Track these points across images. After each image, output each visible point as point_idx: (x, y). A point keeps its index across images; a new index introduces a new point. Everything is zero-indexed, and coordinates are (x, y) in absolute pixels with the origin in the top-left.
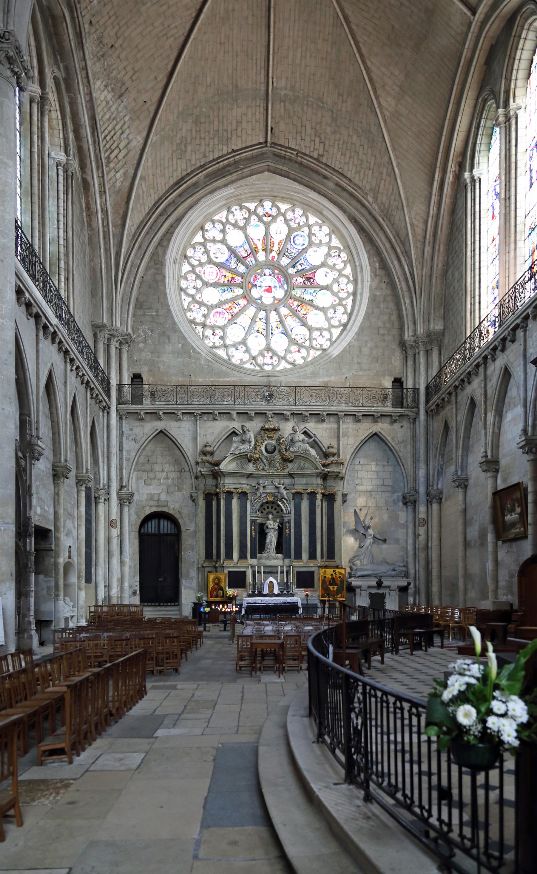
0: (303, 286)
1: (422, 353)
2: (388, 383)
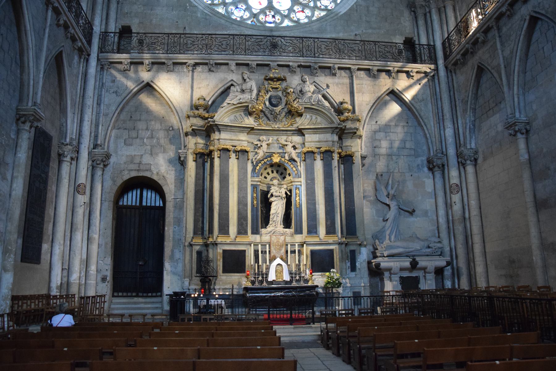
1: (434, 11)
2: (399, 40)
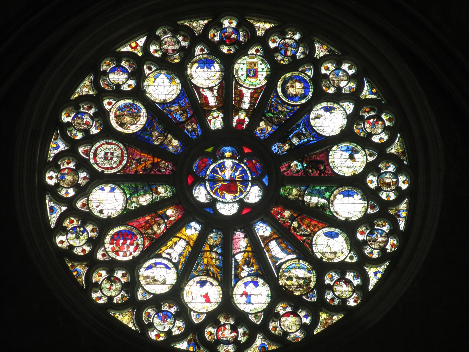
0: (304, 180)
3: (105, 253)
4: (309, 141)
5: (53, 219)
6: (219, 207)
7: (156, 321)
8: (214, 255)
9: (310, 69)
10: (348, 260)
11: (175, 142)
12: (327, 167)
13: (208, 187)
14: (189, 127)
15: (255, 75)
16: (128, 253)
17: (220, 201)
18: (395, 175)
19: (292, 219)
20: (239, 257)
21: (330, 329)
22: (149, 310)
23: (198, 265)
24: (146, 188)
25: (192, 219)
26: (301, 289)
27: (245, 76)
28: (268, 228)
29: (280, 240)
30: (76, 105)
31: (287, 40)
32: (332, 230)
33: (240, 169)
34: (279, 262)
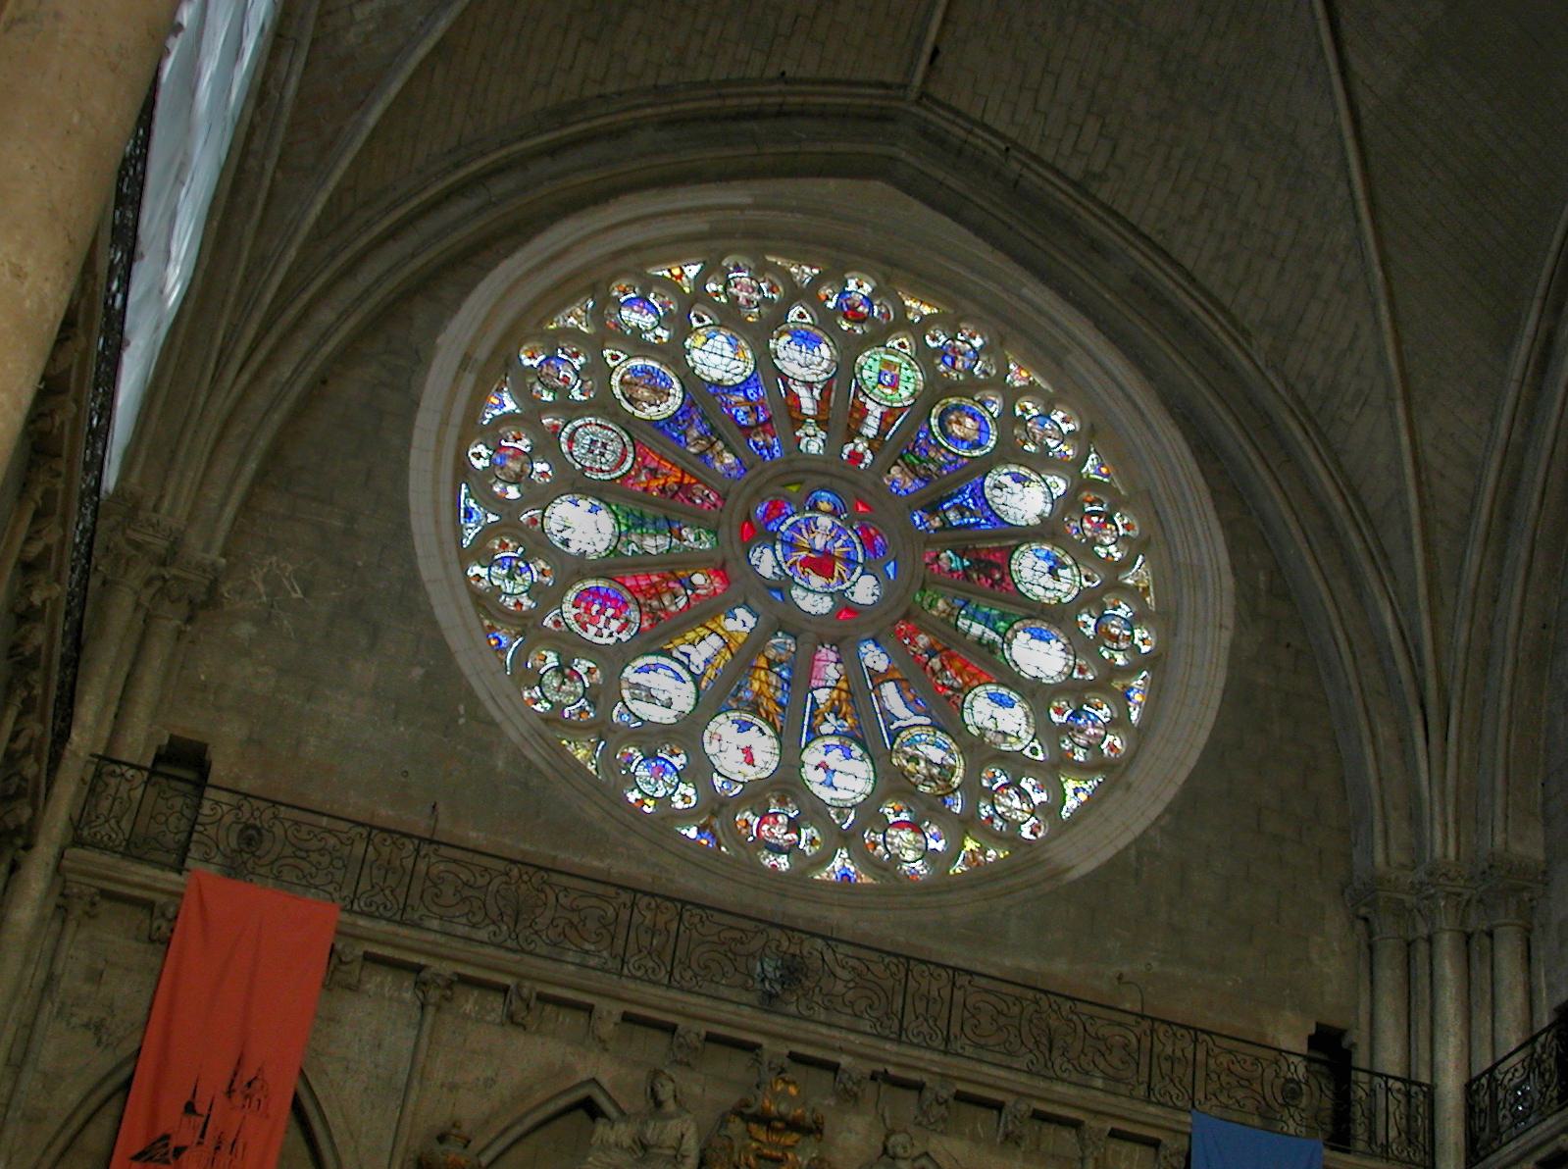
3: (561, 619)
4: (978, 524)
5: (471, 533)
6: (797, 593)
7: (642, 772)
8: (773, 679)
9: (994, 402)
10: (1027, 752)
11: (729, 459)
12: (1008, 579)
13: (779, 554)
14: (760, 440)
15: (894, 385)
16: (606, 632)
17: (798, 584)
18: (1130, 624)
19: (931, 651)
20: (822, 695)
21: (981, 876)
22: (631, 750)
23: (739, 688)
24: (661, 523)
25: (741, 601)
26: (933, 784)
27: (876, 380)
28: (884, 656)
29: (904, 685)
30: (552, 342)
31: (958, 343)
32: (1003, 691)
33: (844, 537)
34: (896, 724)
